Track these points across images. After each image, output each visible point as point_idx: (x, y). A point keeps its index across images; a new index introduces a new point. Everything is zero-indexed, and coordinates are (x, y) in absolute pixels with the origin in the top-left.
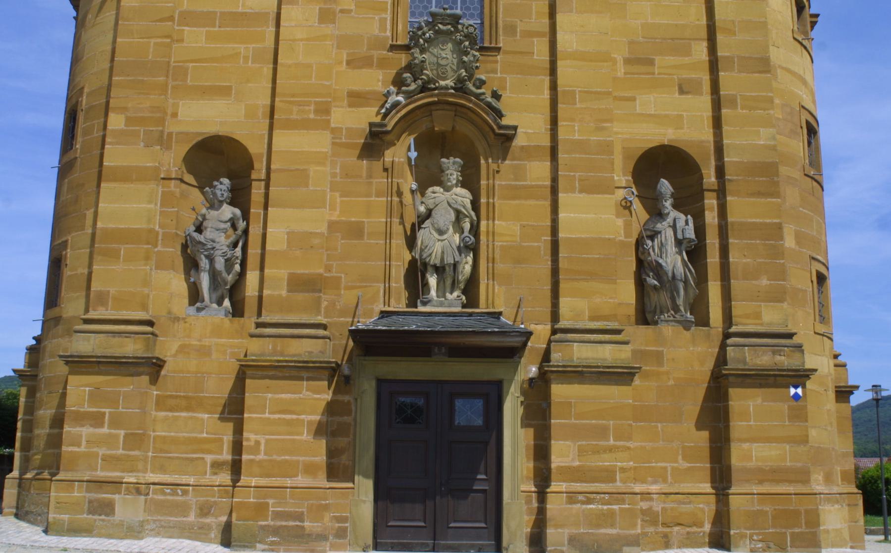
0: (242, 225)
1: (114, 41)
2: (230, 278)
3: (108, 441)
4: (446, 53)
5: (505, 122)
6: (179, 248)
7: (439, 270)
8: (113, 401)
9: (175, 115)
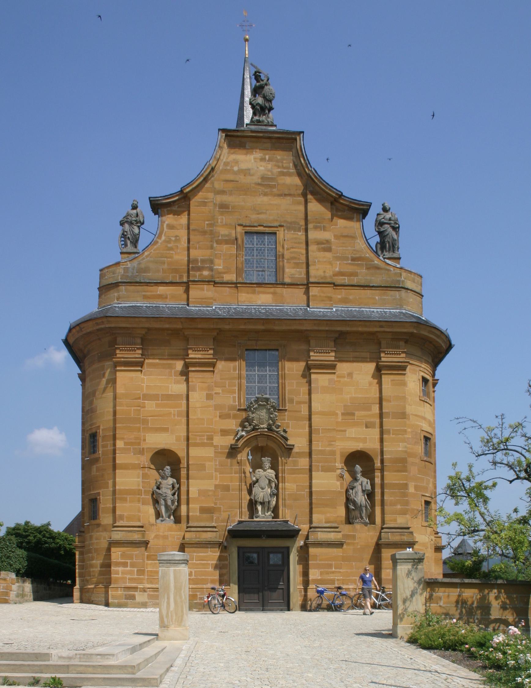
0: (177, 486)
1: (115, 406)
2: (173, 507)
3: (131, 573)
4: (263, 414)
5: (289, 443)
6: (150, 495)
7: (262, 504)
8: (131, 557)
9: (145, 440)
